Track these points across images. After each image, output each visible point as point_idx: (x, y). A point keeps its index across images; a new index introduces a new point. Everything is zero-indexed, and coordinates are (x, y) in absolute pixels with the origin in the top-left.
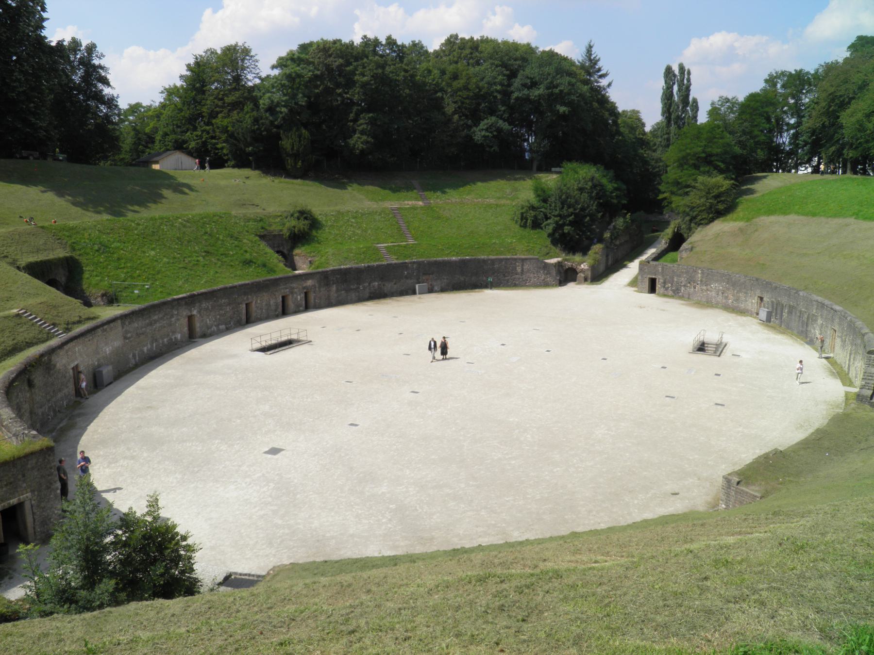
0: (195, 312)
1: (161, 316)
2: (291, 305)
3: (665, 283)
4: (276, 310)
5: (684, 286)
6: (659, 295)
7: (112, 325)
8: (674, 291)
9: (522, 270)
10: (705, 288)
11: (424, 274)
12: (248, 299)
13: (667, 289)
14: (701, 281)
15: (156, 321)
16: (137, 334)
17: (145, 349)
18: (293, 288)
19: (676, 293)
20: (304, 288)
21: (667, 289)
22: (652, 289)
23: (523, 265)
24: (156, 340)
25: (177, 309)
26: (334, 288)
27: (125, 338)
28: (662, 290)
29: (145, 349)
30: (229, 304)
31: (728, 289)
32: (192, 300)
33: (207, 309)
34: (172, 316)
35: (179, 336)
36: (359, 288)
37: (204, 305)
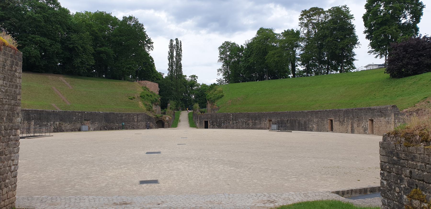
3: (213, 123)
5: (223, 123)
6: (210, 128)
8: (218, 126)
9: (137, 120)
10: (235, 122)
11: (85, 120)
13: (214, 125)
14: (233, 119)
19: (220, 127)
21: (214, 125)
22: (206, 127)
23: (138, 117)
26: (33, 123)
28: (212, 126)
31: (249, 120)
36: (48, 124)
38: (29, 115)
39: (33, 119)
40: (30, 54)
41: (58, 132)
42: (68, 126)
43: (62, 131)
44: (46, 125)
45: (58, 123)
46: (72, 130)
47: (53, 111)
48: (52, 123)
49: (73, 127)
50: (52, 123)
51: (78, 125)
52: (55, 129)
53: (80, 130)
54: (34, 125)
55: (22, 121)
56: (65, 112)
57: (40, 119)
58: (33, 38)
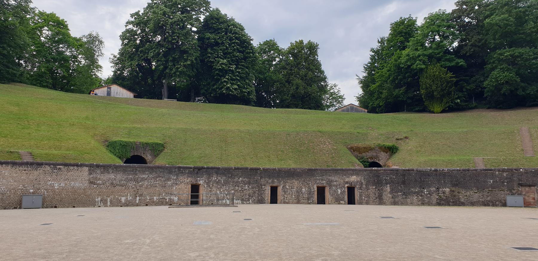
0: (201, 182)
1: (151, 176)
2: (328, 196)
4: (308, 199)
7: (72, 168)
12: (273, 182)
15: (143, 179)
16: (112, 184)
17: (123, 199)
18: (332, 181)
20: (347, 183)
24: (141, 195)
25: (177, 175)
26: (388, 188)
27: (91, 183)
29: (123, 199)
30: (249, 183)
32: (198, 171)
33: (217, 183)
34: (169, 179)
35: (176, 199)
36: (422, 192)
37: (214, 178)
38: (379, 177)
39: (387, 184)
40: (497, 81)
41: (449, 205)
42: (476, 196)
43: (457, 203)
44: (417, 193)
45: (447, 190)
46: (486, 204)
47: (436, 170)
48: (433, 189)
49: (489, 199)
50: (433, 189)
51: (501, 195)
52: (440, 199)
53: (504, 205)
54: (391, 193)
55: (364, 186)
56: (464, 170)
57: (404, 183)
58: (501, 54)
